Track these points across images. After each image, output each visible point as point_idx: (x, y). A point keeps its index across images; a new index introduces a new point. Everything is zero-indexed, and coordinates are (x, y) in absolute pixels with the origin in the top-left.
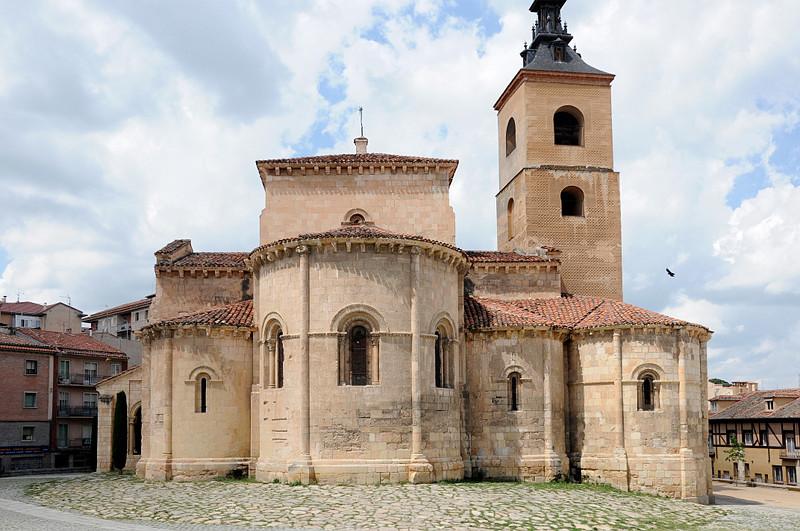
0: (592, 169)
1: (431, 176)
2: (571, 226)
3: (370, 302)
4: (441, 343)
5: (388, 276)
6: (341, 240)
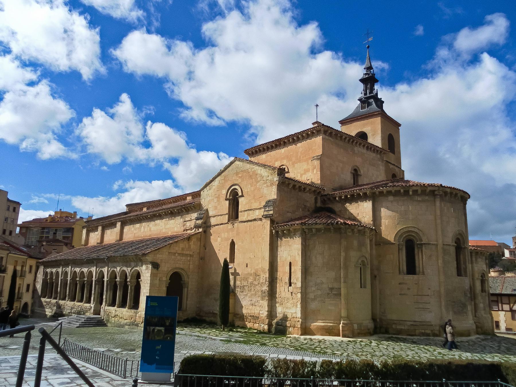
1: (379, 156)
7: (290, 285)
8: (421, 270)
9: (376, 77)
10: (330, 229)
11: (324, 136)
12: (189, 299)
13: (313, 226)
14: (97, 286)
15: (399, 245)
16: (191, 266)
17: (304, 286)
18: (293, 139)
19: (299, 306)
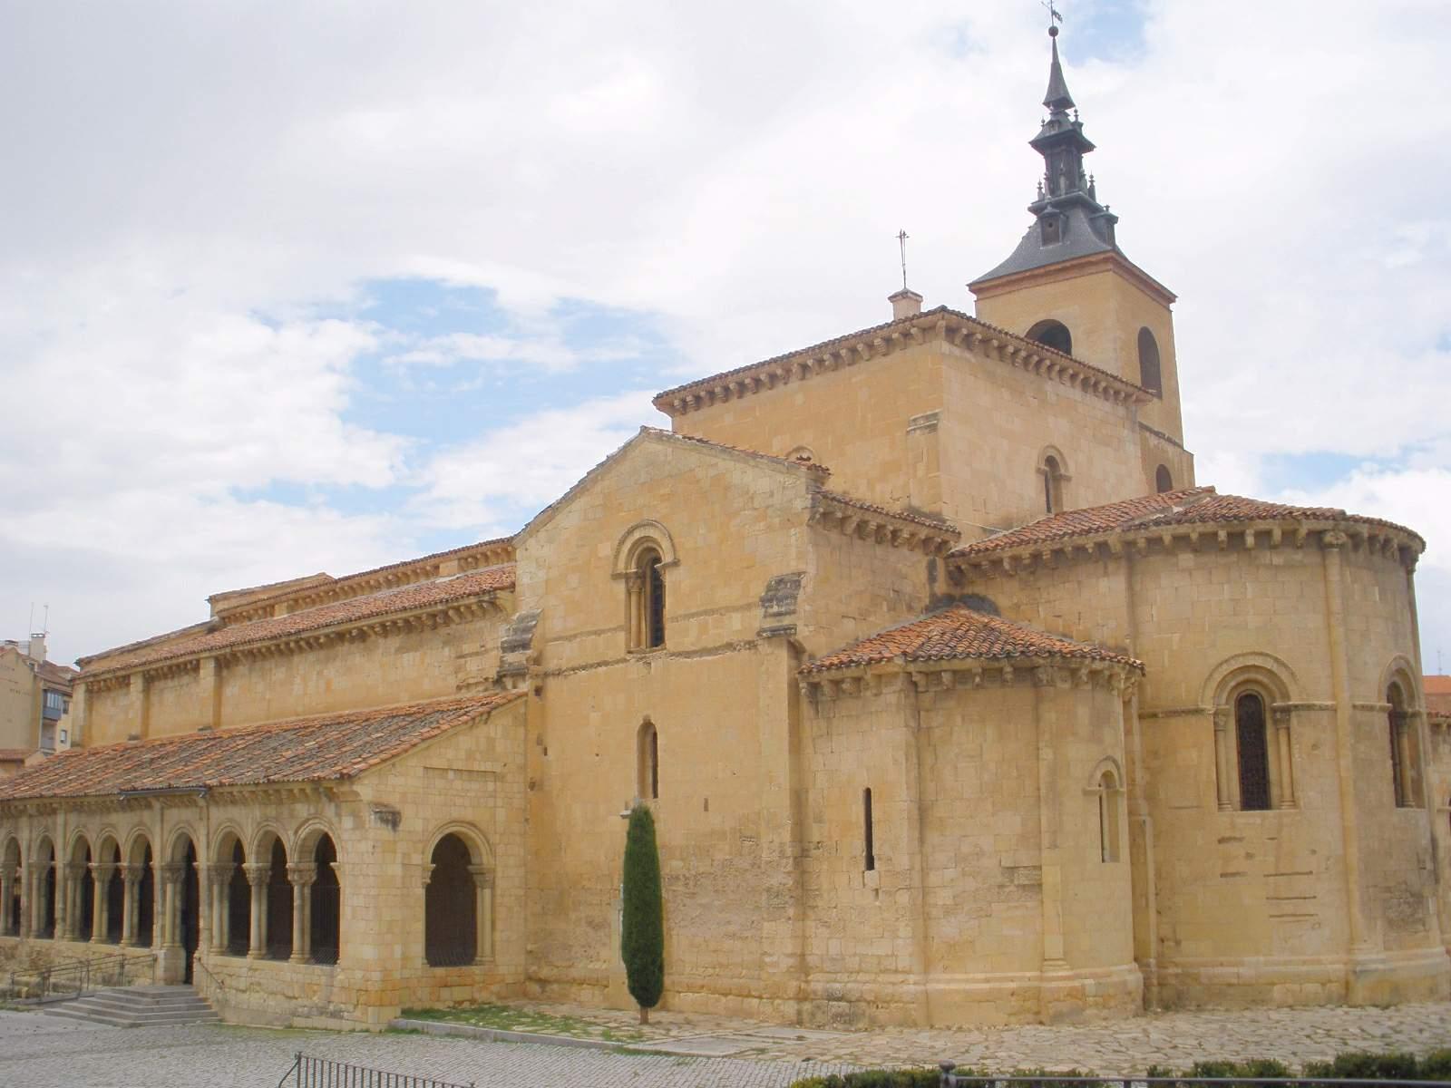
1: (1121, 411)
7: (870, 865)
8: (1287, 792)
9: (1087, 133)
10: (1001, 670)
11: (946, 347)
12: (499, 925)
13: (945, 665)
14: (169, 887)
15: (1216, 714)
16: (501, 815)
17: (918, 867)
18: (836, 356)
19: (904, 931)
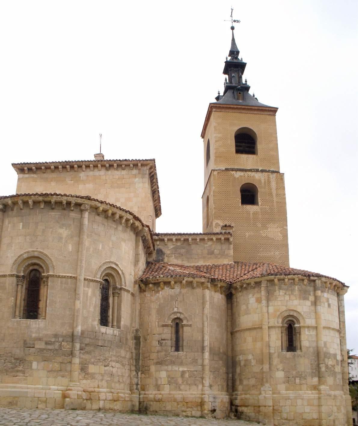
0: (262, 171)
1: (135, 171)
2: (248, 213)
3: (43, 249)
4: (108, 287)
5: (60, 227)
6: (25, 199)
